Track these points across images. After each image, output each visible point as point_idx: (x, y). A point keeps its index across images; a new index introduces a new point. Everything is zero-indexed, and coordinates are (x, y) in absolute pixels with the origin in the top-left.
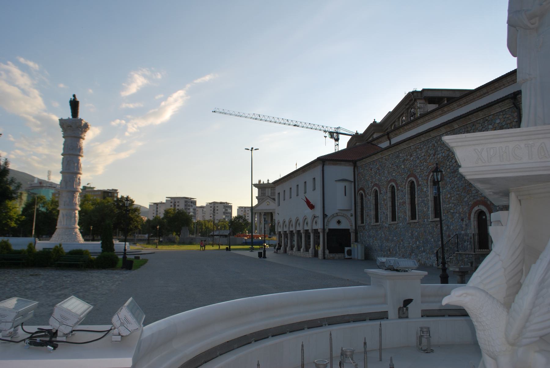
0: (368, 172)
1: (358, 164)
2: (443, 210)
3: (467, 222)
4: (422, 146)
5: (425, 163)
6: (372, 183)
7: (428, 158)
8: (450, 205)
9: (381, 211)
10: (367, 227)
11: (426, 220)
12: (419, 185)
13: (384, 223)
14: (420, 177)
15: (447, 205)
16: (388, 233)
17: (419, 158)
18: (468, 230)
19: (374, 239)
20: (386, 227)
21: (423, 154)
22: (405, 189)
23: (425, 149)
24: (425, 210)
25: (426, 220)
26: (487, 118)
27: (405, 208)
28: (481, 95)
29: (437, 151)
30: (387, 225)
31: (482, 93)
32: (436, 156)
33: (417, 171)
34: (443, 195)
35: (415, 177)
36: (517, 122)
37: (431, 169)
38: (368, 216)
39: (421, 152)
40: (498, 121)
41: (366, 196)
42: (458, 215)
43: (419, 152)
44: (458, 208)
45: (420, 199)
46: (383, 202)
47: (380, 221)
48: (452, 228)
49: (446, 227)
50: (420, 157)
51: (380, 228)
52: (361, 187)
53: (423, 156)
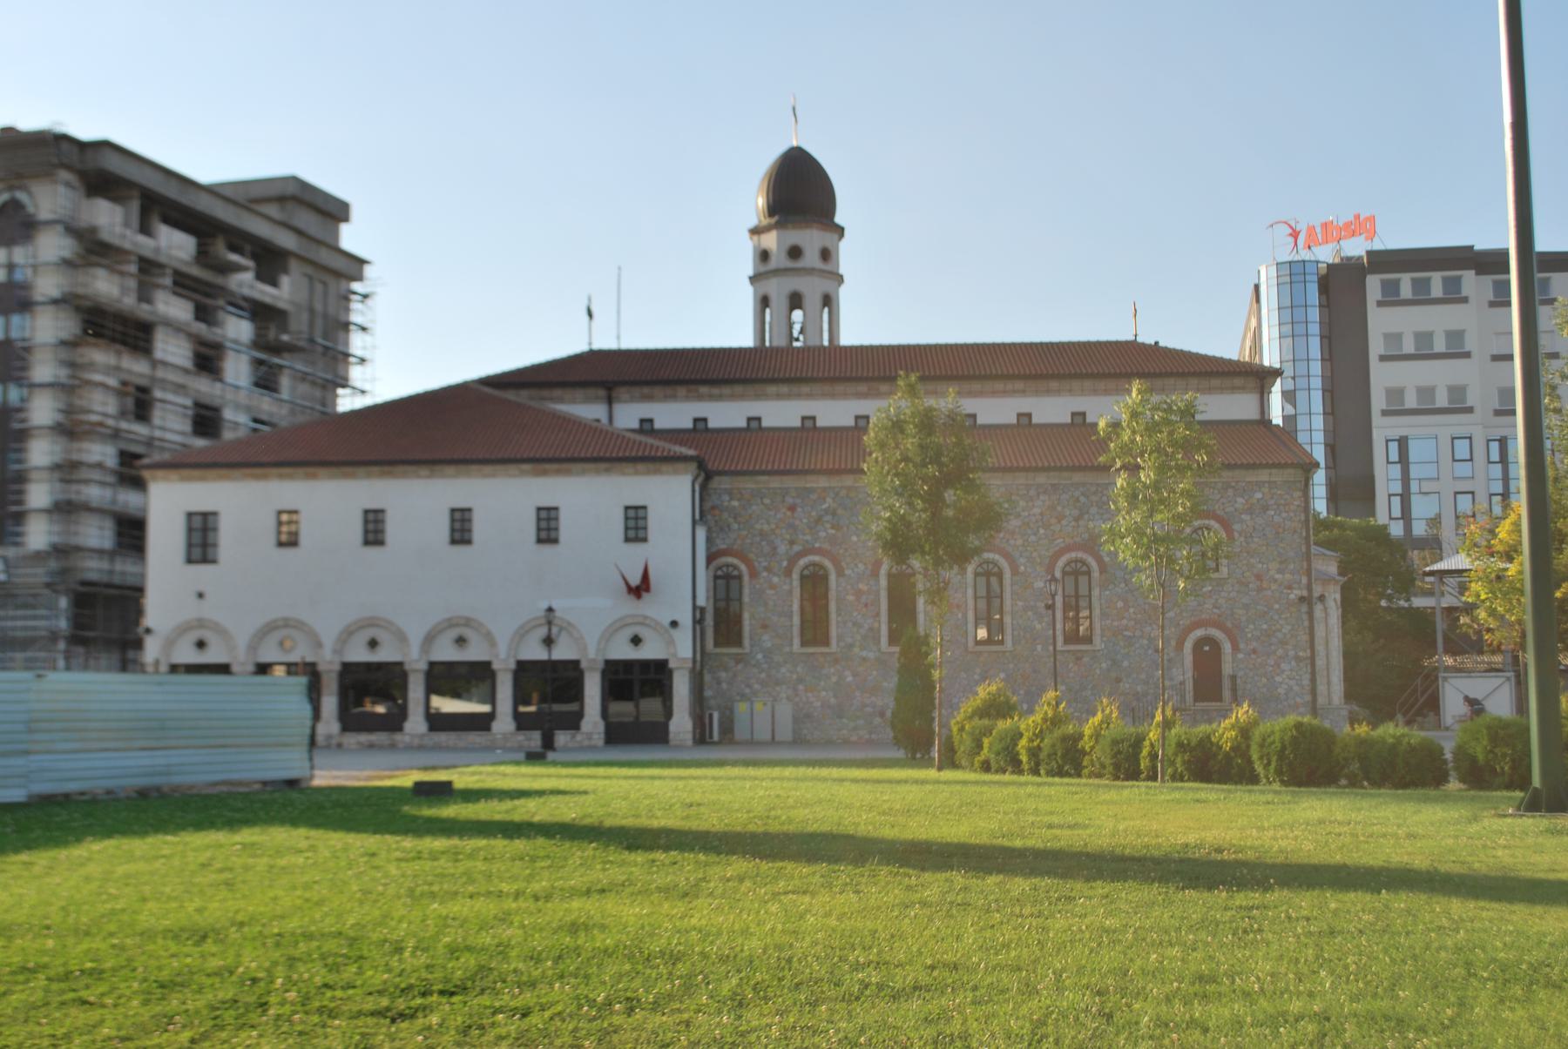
0: (772, 513)
1: (719, 483)
2: (1102, 630)
3: (1172, 654)
4: (1032, 492)
5: (1042, 531)
6: (792, 543)
7: (1053, 521)
8: (1125, 622)
9: (839, 619)
10: (760, 656)
11: (1039, 648)
12: (1015, 572)
13: (856, 650)
14: (1021, 556)
15: (1113, 620)
16: (875, 673)
17: (1020, 516)
18: (1174, 670)
19: (801, 687)
20: (864, 659)
21: (1037, 511)
22: (959, 577)
23: (1044, 501)
24: (1038, 627)
25: (1039, 648)
26: (1233, 484)
27: (960, 616)
28: (1005, 392)
29: (1088, 513)
30: (871, 655)
31: (1010, 386)
32: (1081, 523)
33: (1012, 542)
34: (1103, 601)
35: (1007, 556)
36: (1298, 506)
37: (1062, 545)
38: (765, 627)
39: (1030, 504)
40: (1259, 495)
41: (754, 574)
42: (1145, 642)
43: (1022, 503)
44: (1149, 629)
45: (1020, 603)
46: (851, 598)
47: (838, 642)
48: (1126, 664)
49: (1109, 662)
50: (1026, 514)
51: (836, 661)
52: (723, 547)
53: (1034, 515)
